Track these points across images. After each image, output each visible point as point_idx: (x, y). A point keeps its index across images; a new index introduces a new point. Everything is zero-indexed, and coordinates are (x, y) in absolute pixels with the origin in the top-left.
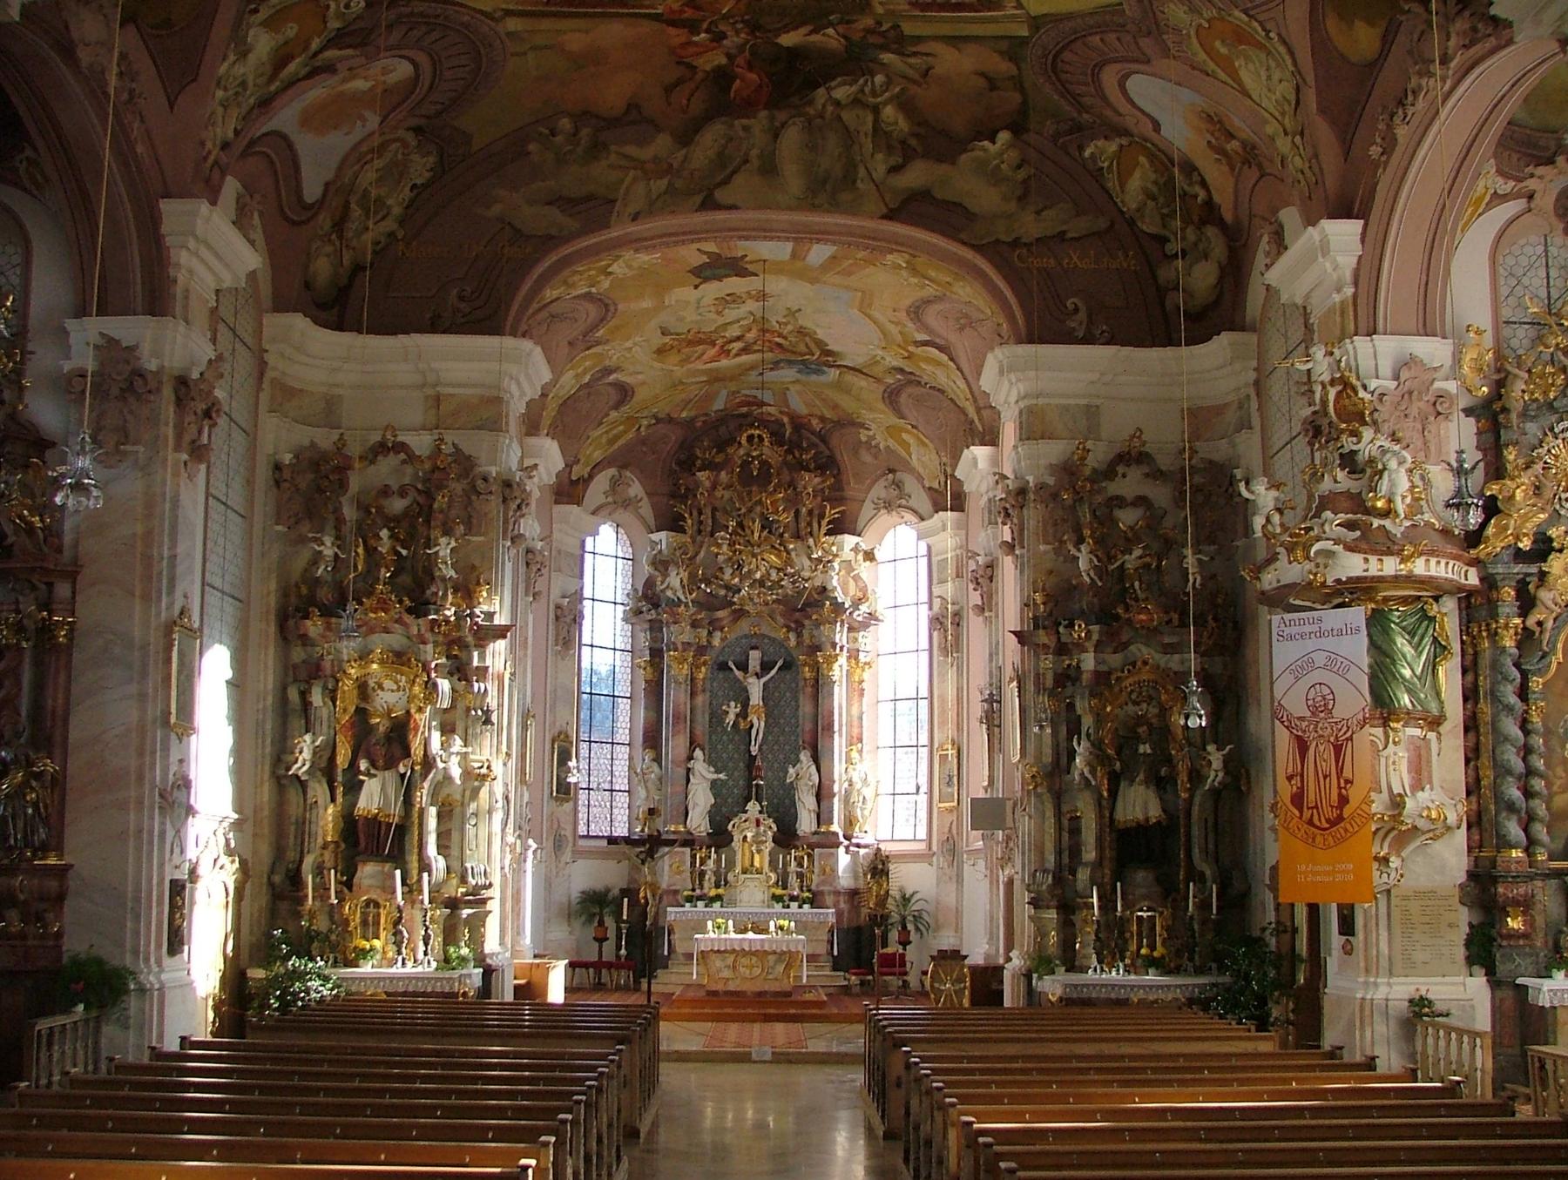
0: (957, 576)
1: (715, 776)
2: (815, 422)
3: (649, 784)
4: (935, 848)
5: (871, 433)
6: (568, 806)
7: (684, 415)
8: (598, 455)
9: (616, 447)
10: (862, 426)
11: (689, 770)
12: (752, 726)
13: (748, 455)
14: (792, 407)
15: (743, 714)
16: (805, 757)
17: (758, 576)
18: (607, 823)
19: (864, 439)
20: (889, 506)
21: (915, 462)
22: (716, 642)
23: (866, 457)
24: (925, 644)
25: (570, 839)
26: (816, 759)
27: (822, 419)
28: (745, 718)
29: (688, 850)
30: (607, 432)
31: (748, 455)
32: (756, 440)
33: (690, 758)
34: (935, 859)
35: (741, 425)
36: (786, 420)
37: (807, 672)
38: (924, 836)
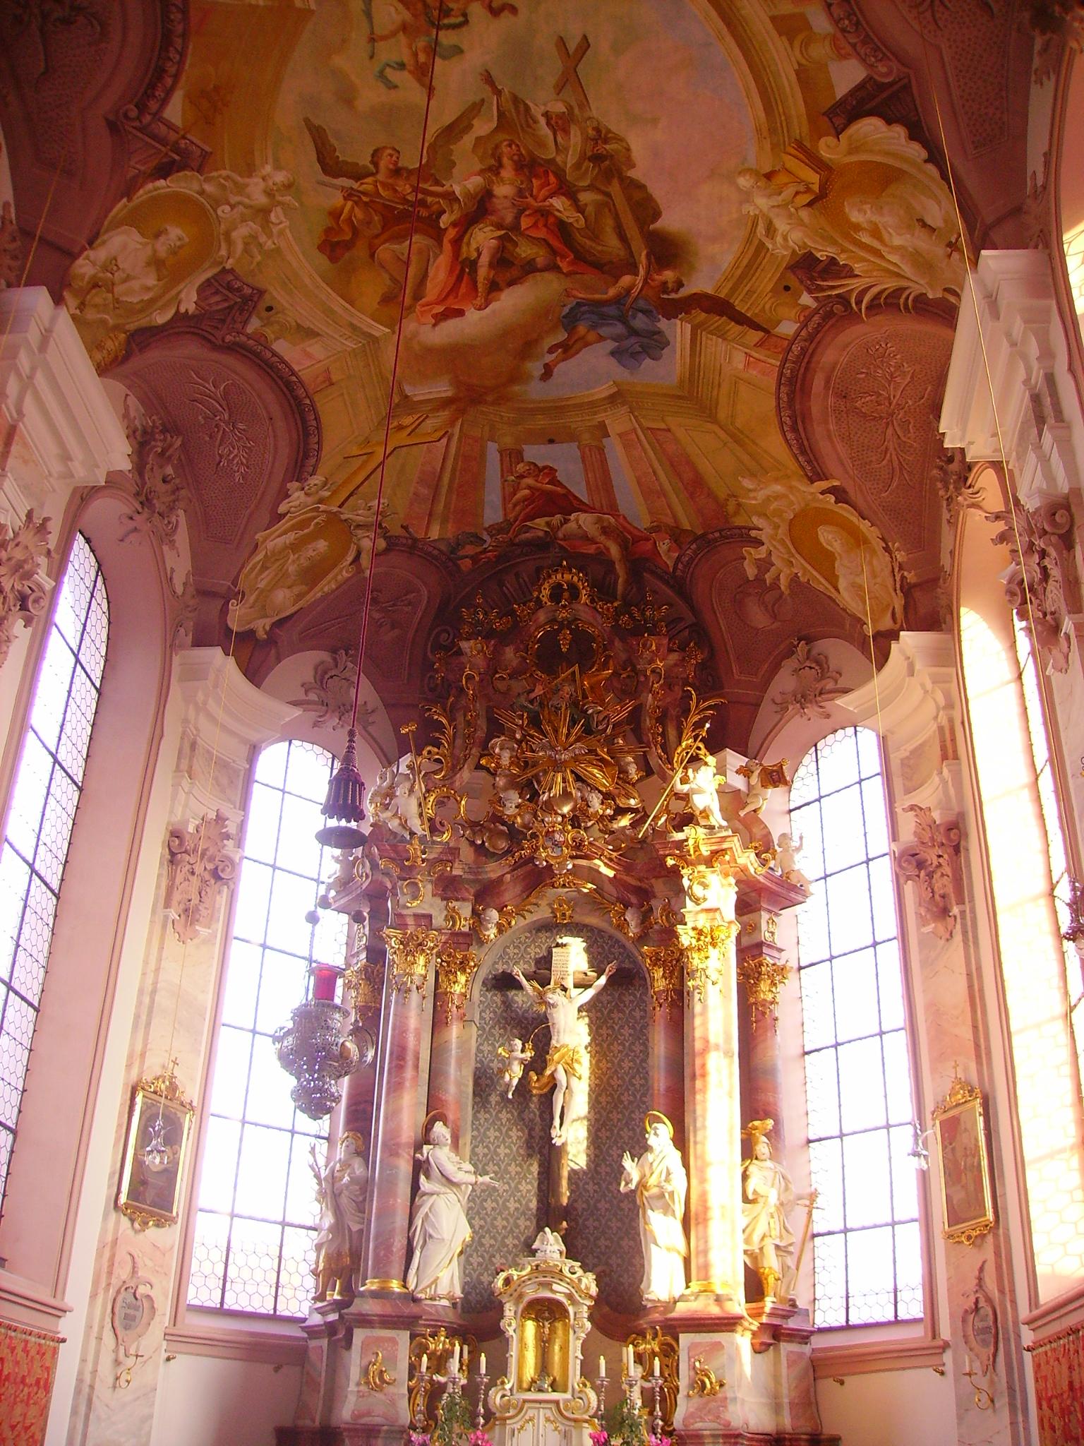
0: (944, 757)
1: (472, 1178)
2: (663, 547)
3: (344, 1200)
4: (945, 1332)
5: (761, 553)
6: (169, 1236)
7: (435, 533)
8: (284, 601)
9: (317, 593)
10: (747, 537)
11: (420, 1167)
12: (554, 1087)
13: (553, 621)
14: (623, 508)
15: (538, 1064)
16: (661, 1135)
17: (566, 809)
18: (269, 1291)
19: (751, 572)
20: (803, 698)
21: (846, 598)
22: (492, 932)
23: (758, 617)
24: (888, 925)
25: (164, 1307)
26: (681, 1141)
27: (677, 535)
28: (540, 1073)
29: (404, 1337)
30: (295, 547)
31: (553, 621)
32: (566, 595)
33: (426, 1138)
34: (948, 1357)
35: (539, 570)
36: (614, 551)
37: (660, 980)
38: (913, 1307)
